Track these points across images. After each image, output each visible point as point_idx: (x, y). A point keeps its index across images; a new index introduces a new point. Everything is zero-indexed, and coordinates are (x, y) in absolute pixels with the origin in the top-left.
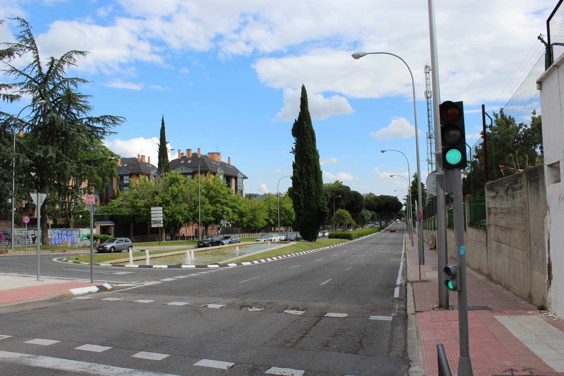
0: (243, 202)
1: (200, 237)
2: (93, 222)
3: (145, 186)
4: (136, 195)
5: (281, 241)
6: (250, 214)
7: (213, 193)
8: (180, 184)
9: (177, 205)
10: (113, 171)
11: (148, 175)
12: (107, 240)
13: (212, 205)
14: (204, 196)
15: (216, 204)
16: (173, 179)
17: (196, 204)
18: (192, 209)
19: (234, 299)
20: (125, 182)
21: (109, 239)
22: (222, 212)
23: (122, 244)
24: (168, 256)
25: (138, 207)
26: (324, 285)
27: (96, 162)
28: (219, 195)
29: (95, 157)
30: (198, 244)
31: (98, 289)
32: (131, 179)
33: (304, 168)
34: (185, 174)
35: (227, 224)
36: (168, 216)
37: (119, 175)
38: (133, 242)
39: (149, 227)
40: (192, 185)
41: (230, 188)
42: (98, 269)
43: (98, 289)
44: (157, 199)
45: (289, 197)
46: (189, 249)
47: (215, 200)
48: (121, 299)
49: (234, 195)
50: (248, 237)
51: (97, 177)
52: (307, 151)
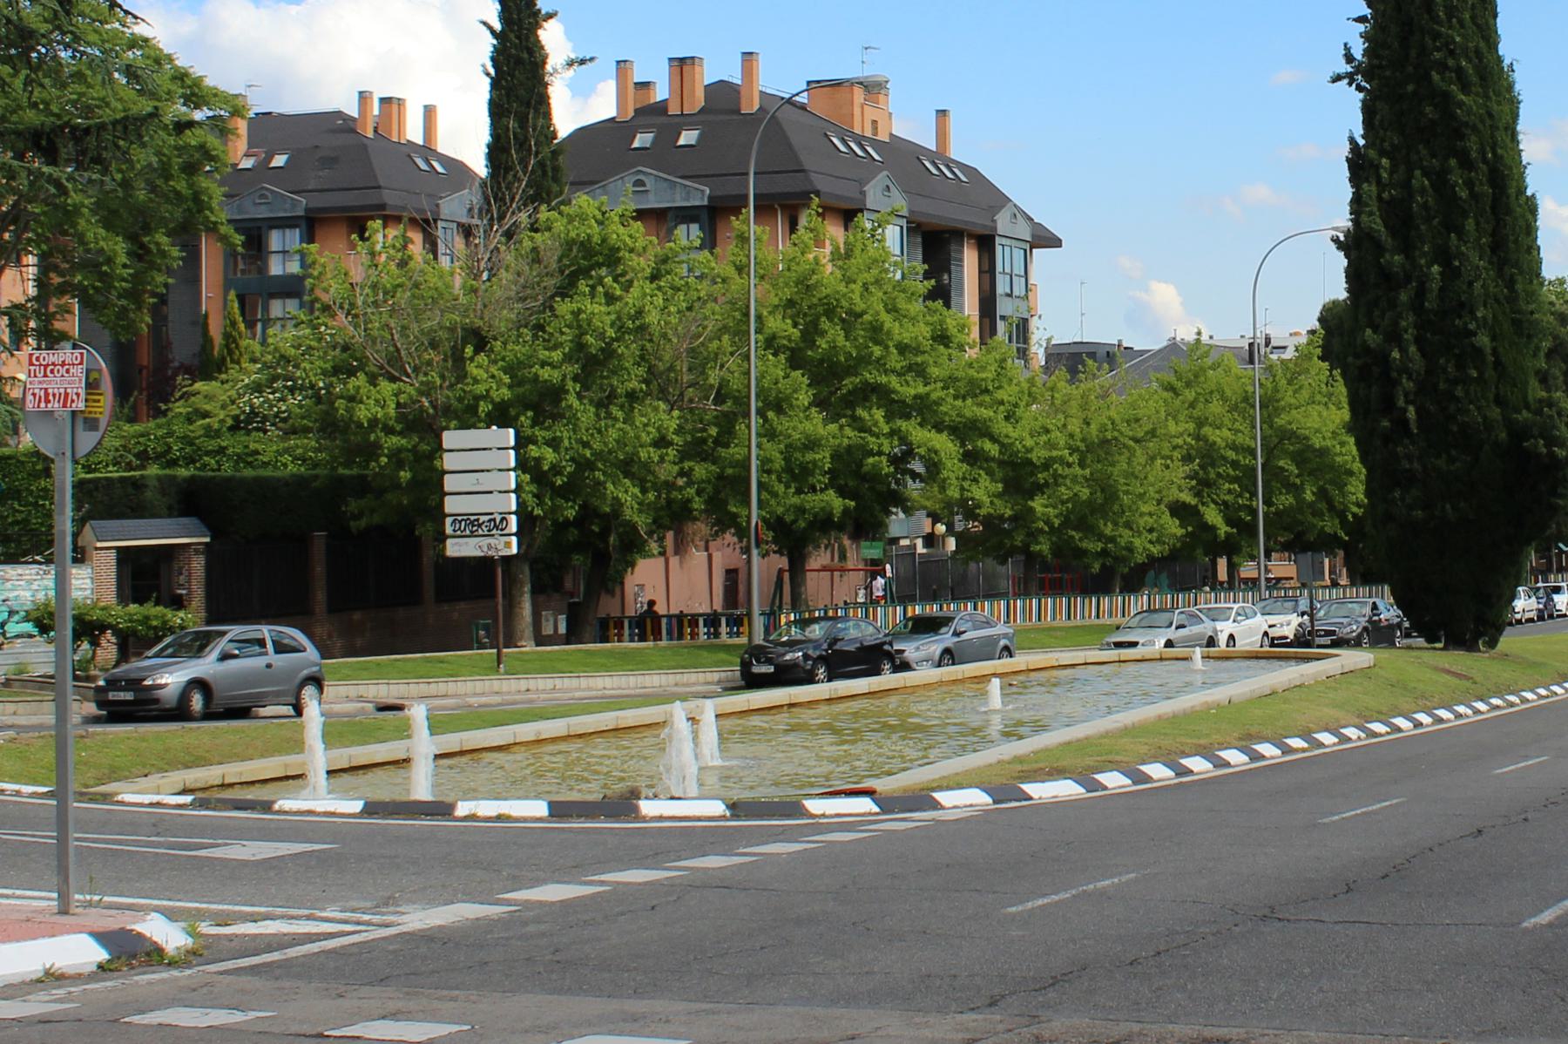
0: (1033, 399)
1: (759, 623)
2: (69, 527)
3: (403, 297)
4: (346, 348)
5: (1277, 649)
6: (1077, 470)
7: (841, 340)
8: (630, 283)
9: (609, 415)
10: (196, 197)
11: (426, 225)
12: (159, 639)
13: (834, 418)
14: (782, 357)
15: (860, 412)
16: (586, 247)
17: (727, 406)
18: (704, 441)
19: (974, 1016)
20: (276, 268)
21: (171, 630)
22: (900, 461)
23: (257, 663)
24: (554, 740)
25: (360, 425)
26: (1550, 925)
27: (91, 141)
28: (877, 351)
29: (88, 111)
30: (745, 666)
31: (102, 955)
32: (314, 247)
33: (1419, 180)
34: (658, 218)
35: (930, 540)
36: (553, 484)
37: (239, 225)
38: (326, 653)
39: (428, 557)
40: (704, 288)
41: (947, 305)
42: (104, 824)
43: (102, 955)
44: (483, 375)
45: (1326, 365)
46: (684, 698)
47: (849, 383)
48: (252, 1015)
49: (972, 353)
50: (1062, 621)
51: (95, 233)
52: (1442, 67)
